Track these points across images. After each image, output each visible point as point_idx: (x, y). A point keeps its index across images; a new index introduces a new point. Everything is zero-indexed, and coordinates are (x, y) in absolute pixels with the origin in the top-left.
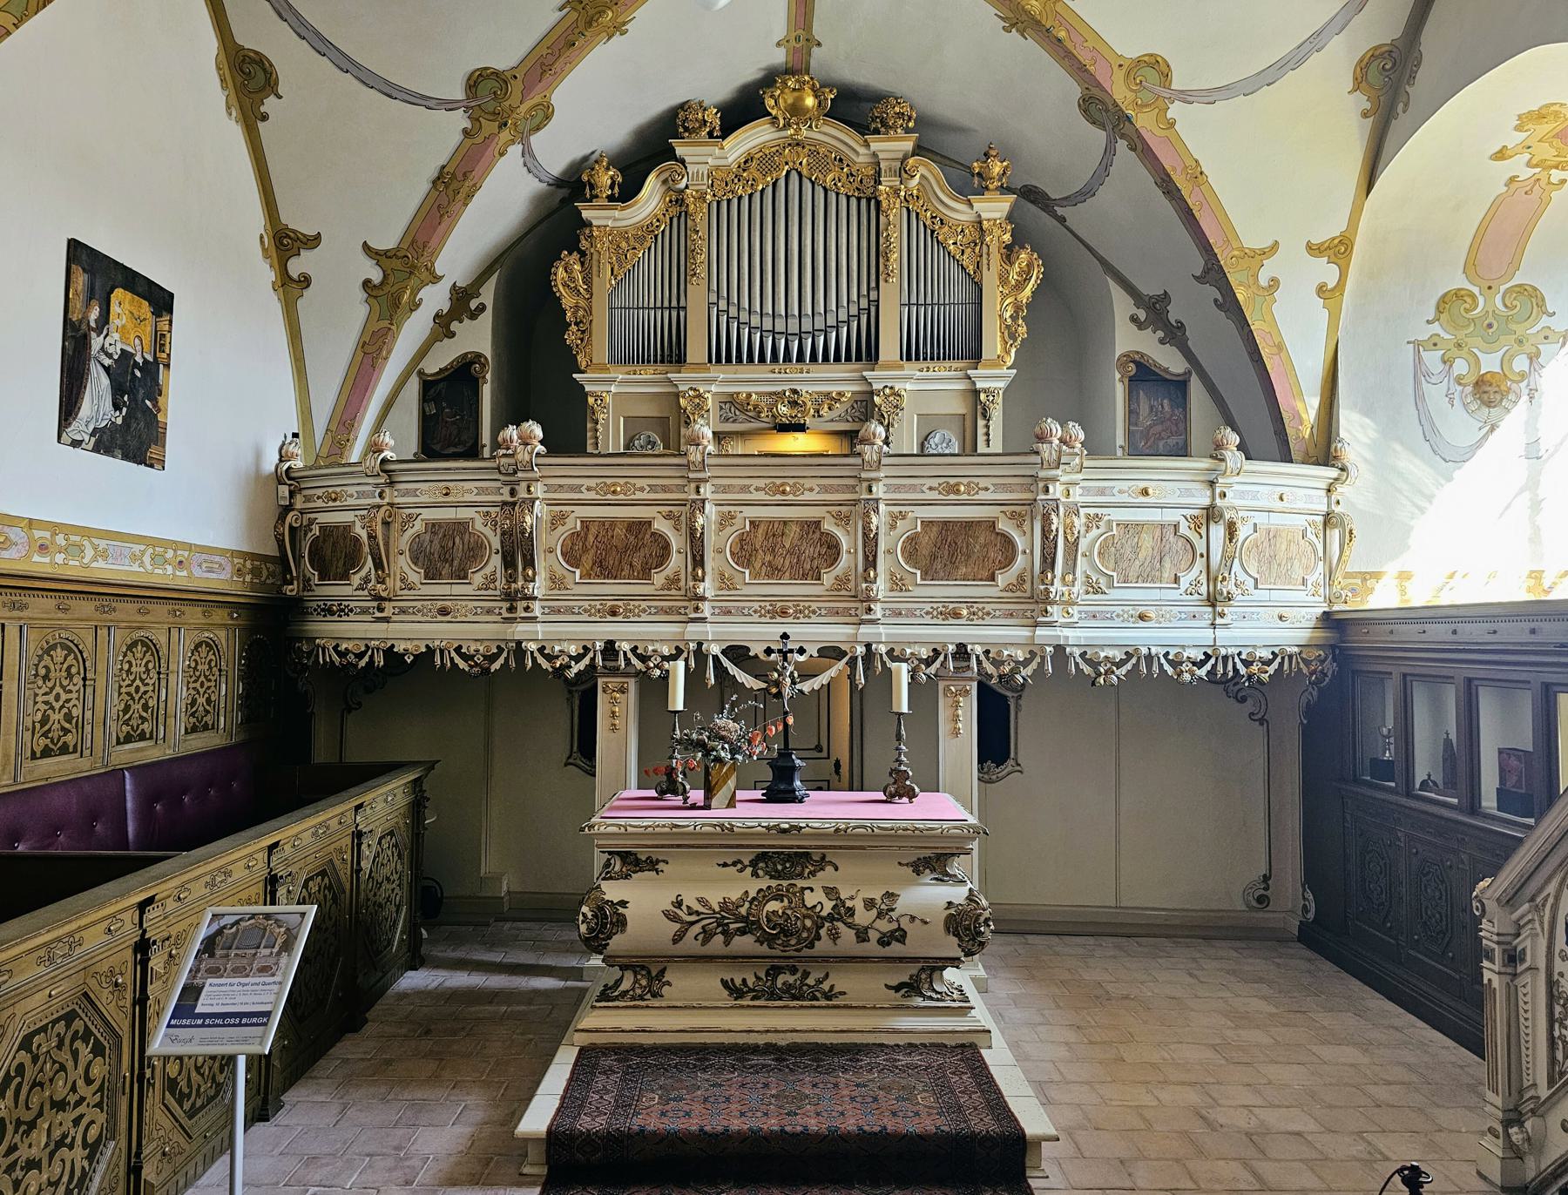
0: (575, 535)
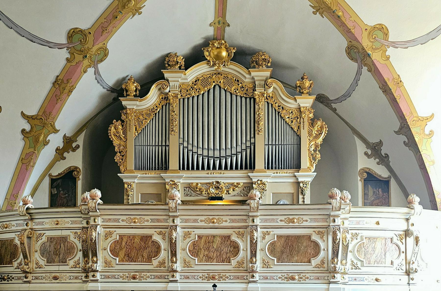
0: (116, 242)
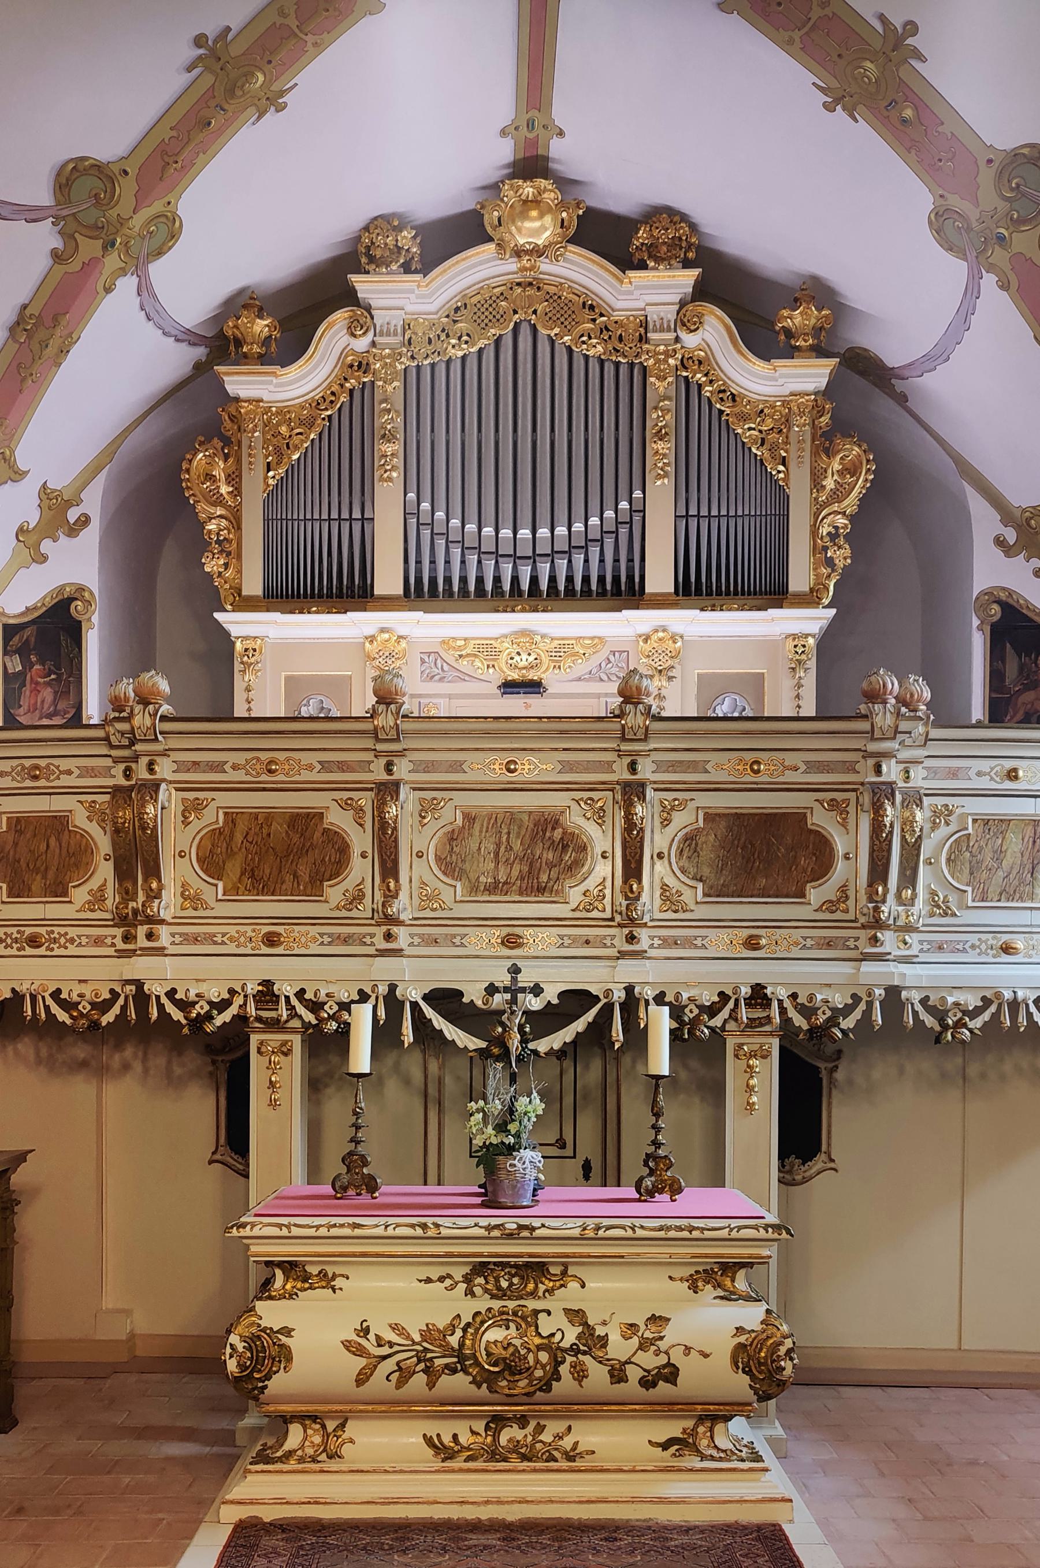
0: (216, 834)
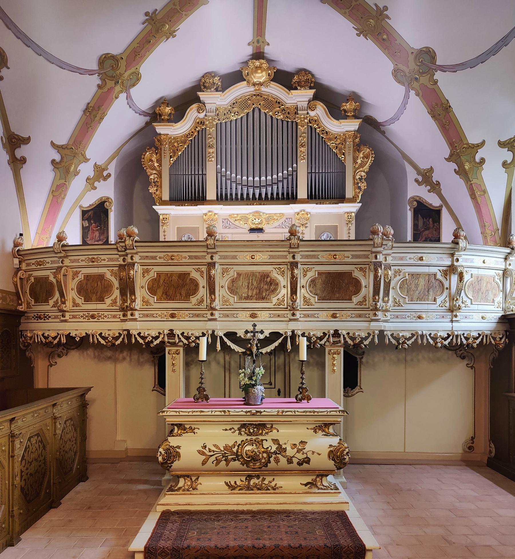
0: (154, 281)
